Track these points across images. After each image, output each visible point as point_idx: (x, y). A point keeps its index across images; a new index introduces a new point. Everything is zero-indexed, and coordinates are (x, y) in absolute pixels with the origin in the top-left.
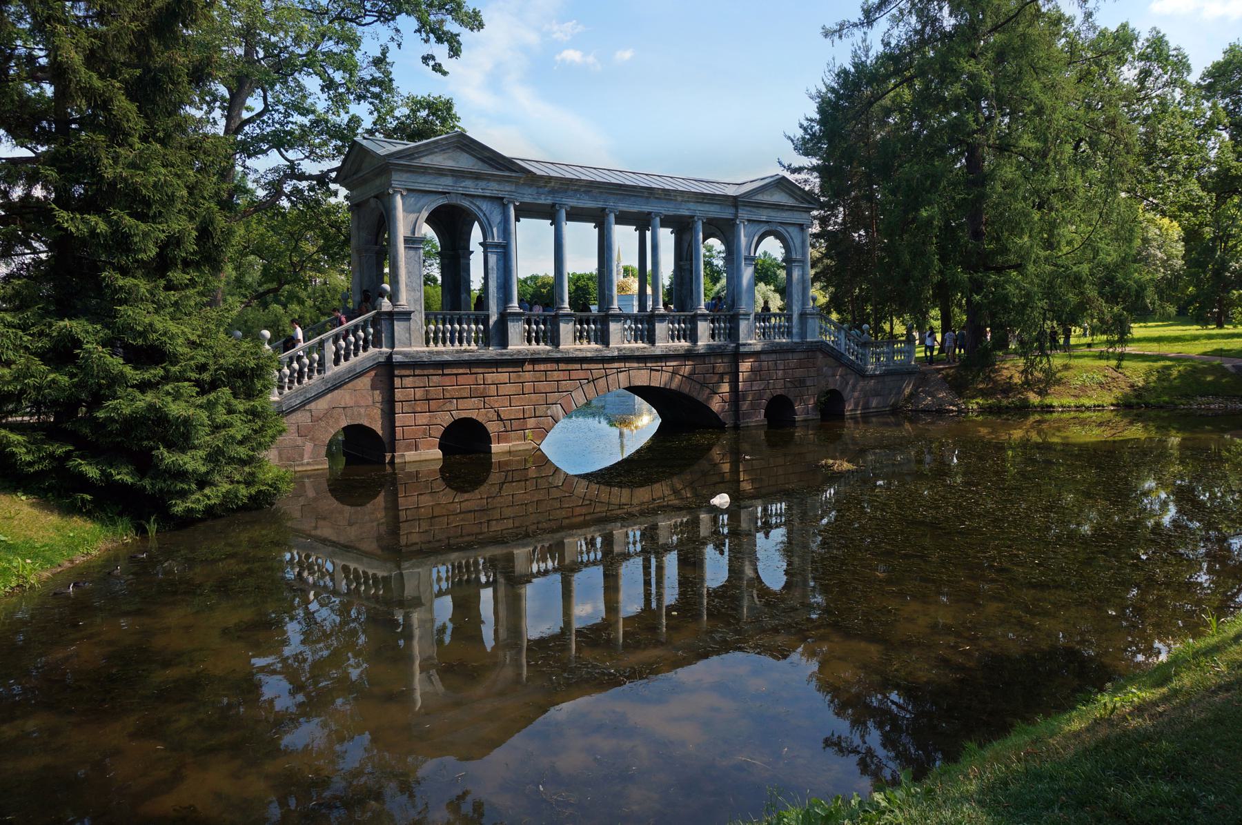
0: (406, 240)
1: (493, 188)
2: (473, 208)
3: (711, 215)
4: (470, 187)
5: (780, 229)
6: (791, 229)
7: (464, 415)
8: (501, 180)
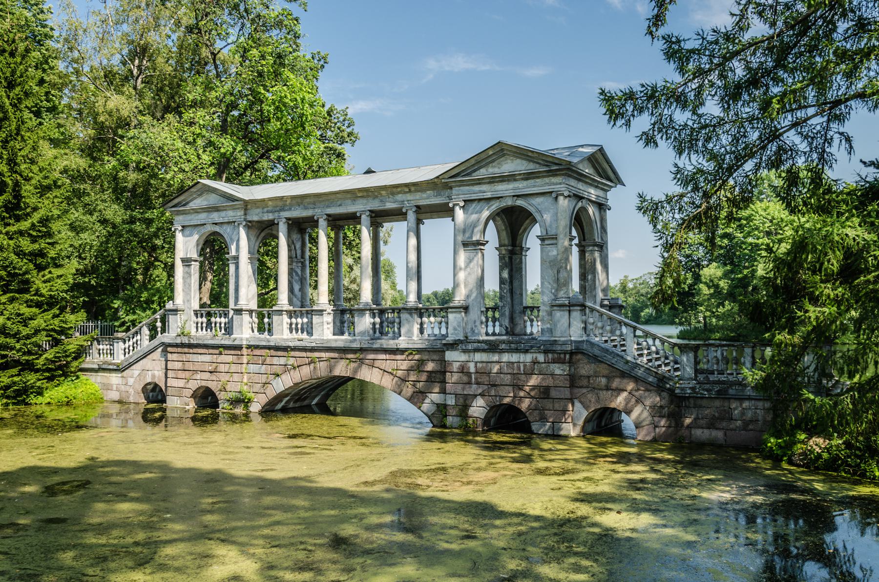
1: (230, 215)
2: (222, 232)
3: (421, 203)
4: (216, 217)
5: (520, 202)
7: (204, 384)
8: (234, 208)
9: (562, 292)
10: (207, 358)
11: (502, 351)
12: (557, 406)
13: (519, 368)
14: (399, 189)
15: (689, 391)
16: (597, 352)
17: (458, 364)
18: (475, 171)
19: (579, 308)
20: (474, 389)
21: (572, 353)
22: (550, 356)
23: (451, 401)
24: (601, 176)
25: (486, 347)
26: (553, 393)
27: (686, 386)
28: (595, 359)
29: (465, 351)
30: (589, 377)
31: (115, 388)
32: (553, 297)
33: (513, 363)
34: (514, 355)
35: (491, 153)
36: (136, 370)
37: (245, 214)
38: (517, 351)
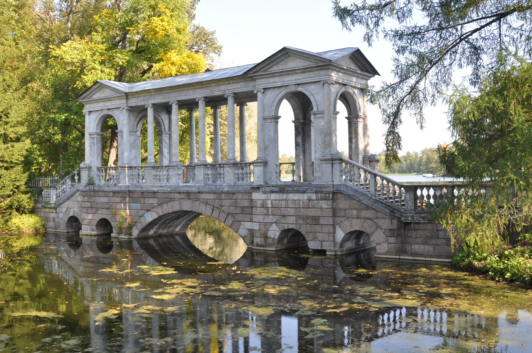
0: (90, 135)
4: (109, 105)
5: (300, 89)
6: (313, 87)
7: (104, 217)
9: (327, 151)
10: (105, 200)
11: (288, 192)
12: (324, 230)
13: (300, 204)
14: (222, 83)
15: (410, 219)
16: (351, 193)
17: (260, 201)
18: (270, 68)
19: (338, 162)
20: (271, 219)
21: (334, 193)
22: (319, 195)
23: (256, 227)
24: (363, 71)
25: (278, 190)
26: (322, 221)
27: (409, 215)
28: (350, 197)
29: (264, 193)
30: (345, 209)
31: (52, 220)
32: (322, 155)
33: (295, 200)
34: (296, 195)
35: (280, 55)
36: (63, 208)
37: (127, 103)
38: (298, 192)
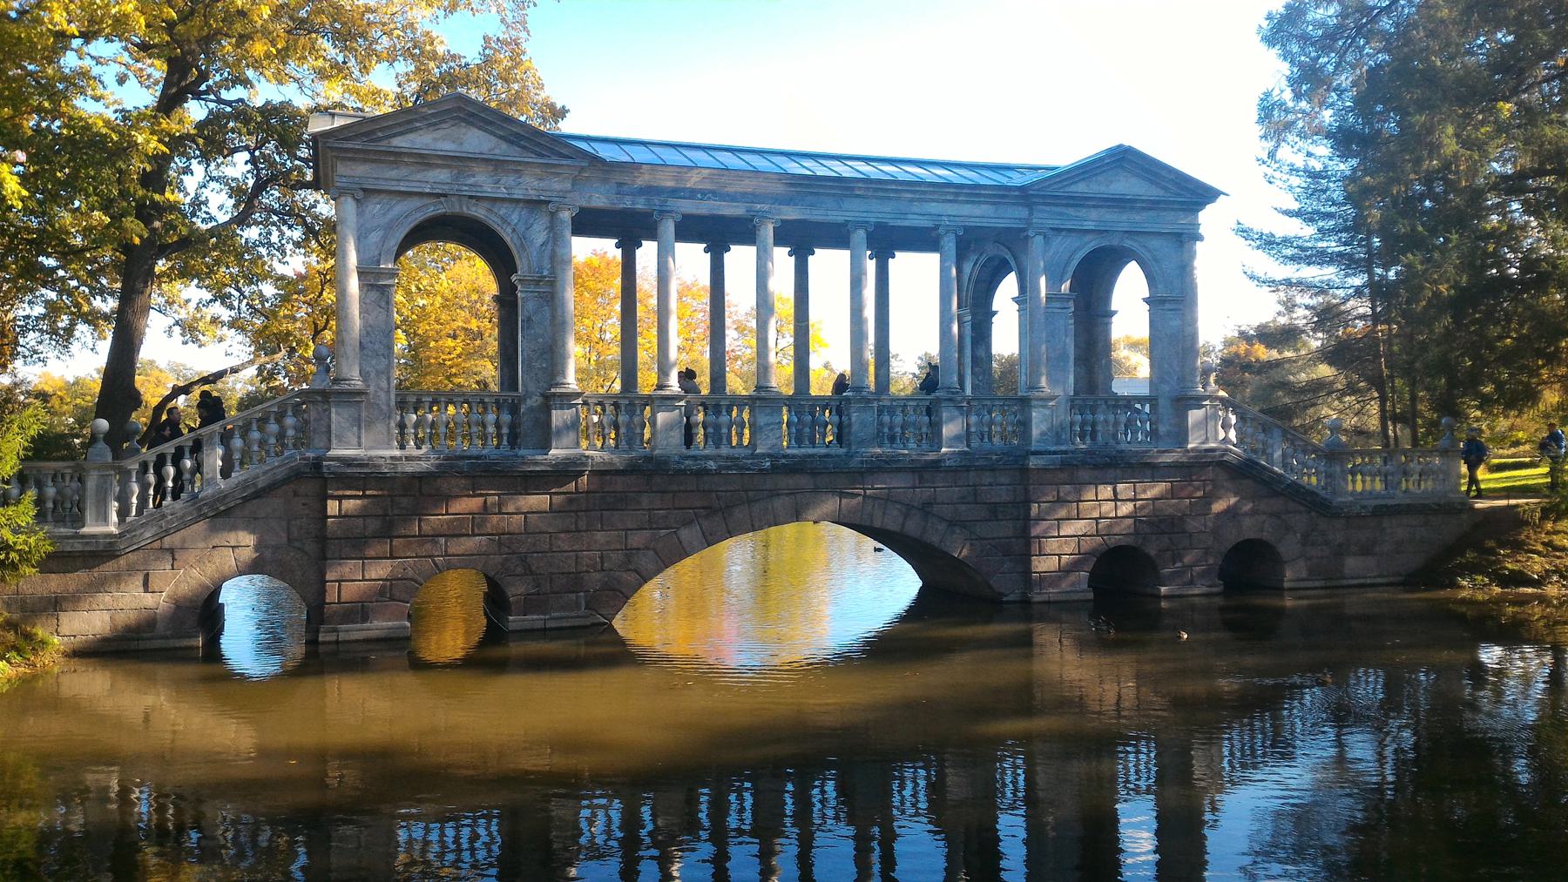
1: (529, 185)
2: (494, 222)
5: (1128, 243)
6: (1155, 243)
